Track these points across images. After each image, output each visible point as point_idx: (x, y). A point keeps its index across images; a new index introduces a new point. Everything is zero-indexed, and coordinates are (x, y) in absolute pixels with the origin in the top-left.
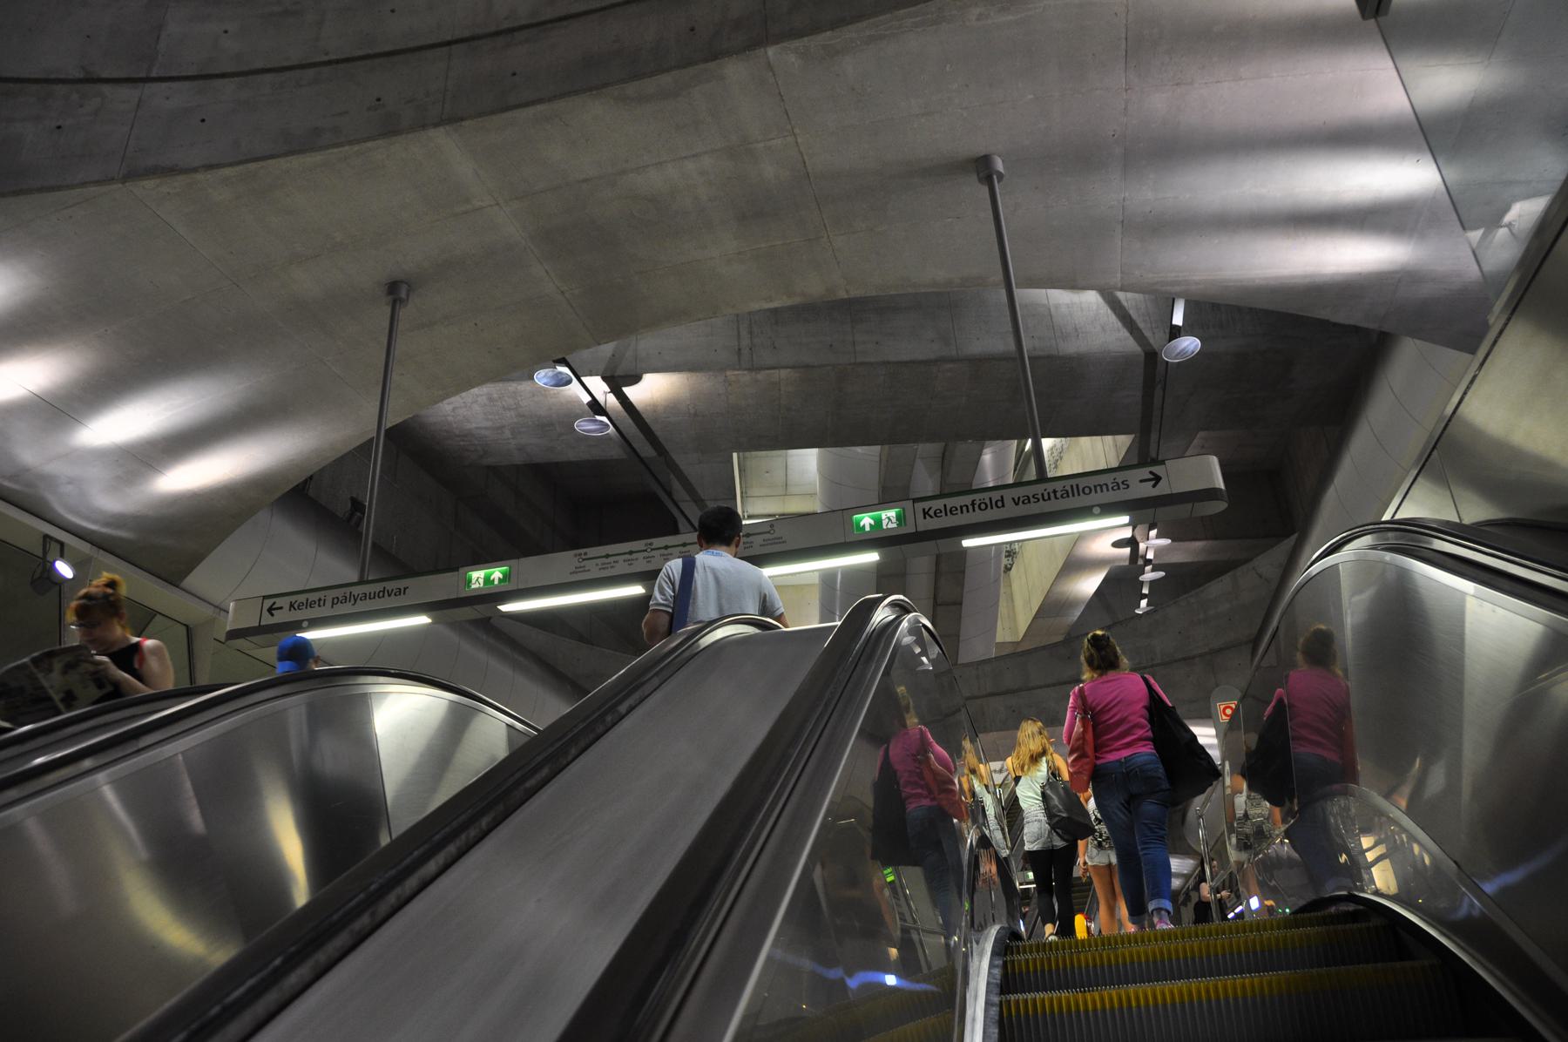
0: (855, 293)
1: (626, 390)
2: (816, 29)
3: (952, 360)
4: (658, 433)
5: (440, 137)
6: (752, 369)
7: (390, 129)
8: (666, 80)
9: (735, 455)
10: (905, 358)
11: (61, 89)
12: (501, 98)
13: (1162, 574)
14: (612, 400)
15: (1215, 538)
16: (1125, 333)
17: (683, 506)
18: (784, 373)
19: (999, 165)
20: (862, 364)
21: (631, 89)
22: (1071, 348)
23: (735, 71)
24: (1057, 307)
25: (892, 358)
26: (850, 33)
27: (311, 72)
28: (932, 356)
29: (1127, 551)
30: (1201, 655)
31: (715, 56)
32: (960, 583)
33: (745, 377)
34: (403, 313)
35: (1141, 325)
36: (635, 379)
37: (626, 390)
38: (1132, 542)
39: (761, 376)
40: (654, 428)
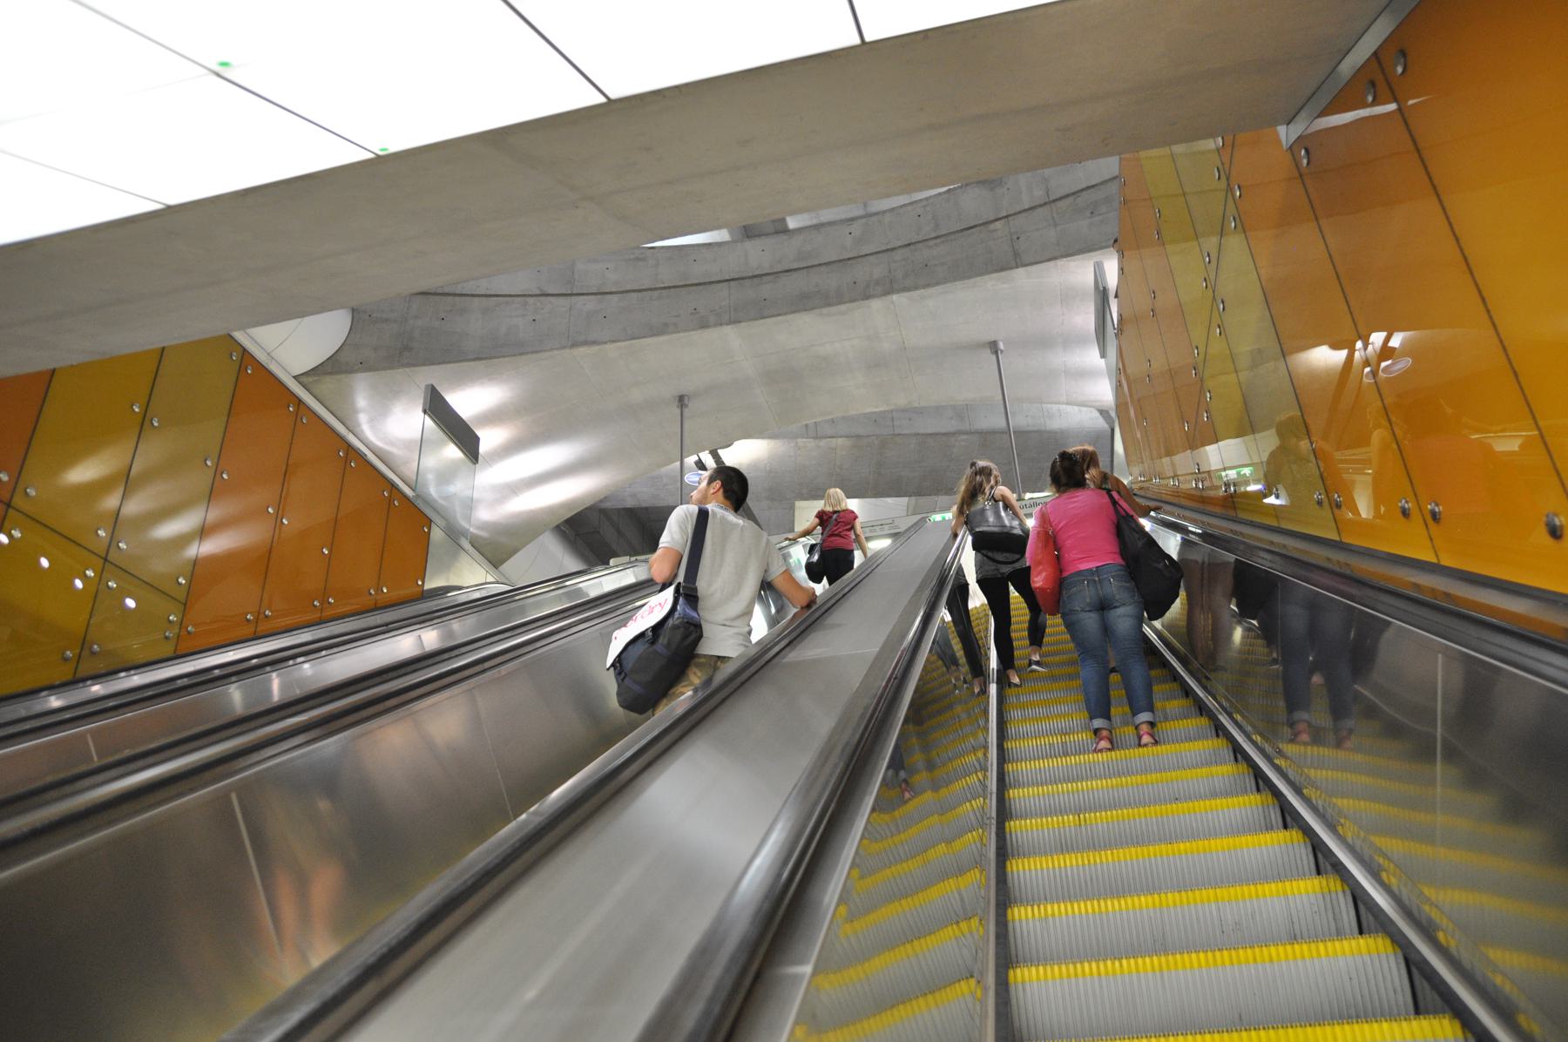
0: (923, 404)
1: (720, 452)
2: (916, 288)
5: (728, 330)
6: (816, 438)
7: (704, 325)
8: (843, 307)
10: (930, 431)
11: (531, 300)
12: (761, 311)
18: (840, 441)
19: (1001, 346)
21: (825, 311)
23: (876, 304)
25: (922, 431)
26: (931, 291)
27: (656, 293)
28: (951, 429)
31: (867, 297)
33: (811, 443)
34: (686, 411)
39: (823, 443)
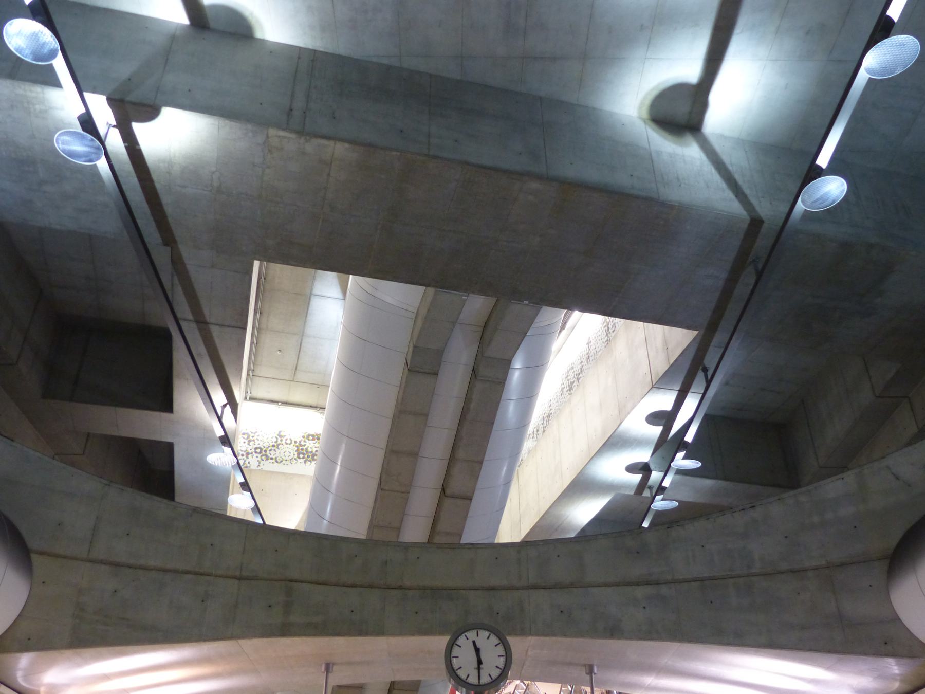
3: (540, 178)
4: (169, 210)
9: (256, 264)
13: (676, 504)
14: (115, 141)
15: (726, 479)
16: (730, 195)
17: (184, 324)
20: (435, 157)
22: (673, 195)
24: (659, 153)
29: (637, 478)
30: (816, 569)
32: (475, 475)
33: (289, 142)
35: (747, 191)
36: (150, 112)
37: (137, 127)
38: (645, 469)
39: (311, 146)
40: (166, 200)
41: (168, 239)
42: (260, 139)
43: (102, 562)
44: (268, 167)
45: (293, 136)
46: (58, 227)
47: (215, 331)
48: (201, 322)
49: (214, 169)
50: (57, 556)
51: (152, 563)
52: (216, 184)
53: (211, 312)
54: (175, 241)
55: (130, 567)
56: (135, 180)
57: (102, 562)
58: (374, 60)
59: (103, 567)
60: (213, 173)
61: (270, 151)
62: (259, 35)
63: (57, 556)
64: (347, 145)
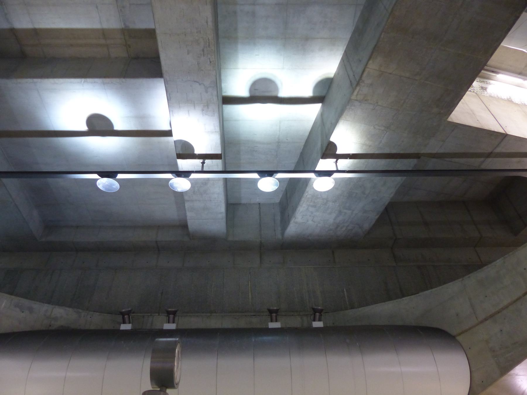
14: (344, 164)
37: (338, 152)
39: (367, 81)
40: (387, 151)
41: (417, 156)
42: (357, 103)
43: (486, 319)
44: (377, 103)
45: (358, 88)
46: (392, 195)
47: (498, 150)
48: (489, 155)
49: (372, 127)
50: (466, 331)
51: (505, 303)
52: (383, 128)
53: (486, 148)
54: (418, 154)
55: (498, 312)
56: (371, 161)
57: (486, 319)
58: (356, 20)
59: (488, 322)
60: (375, 128)
61: (366, 100)
62: (332, 76)
63: (466, 331)
64: (371, 62)
